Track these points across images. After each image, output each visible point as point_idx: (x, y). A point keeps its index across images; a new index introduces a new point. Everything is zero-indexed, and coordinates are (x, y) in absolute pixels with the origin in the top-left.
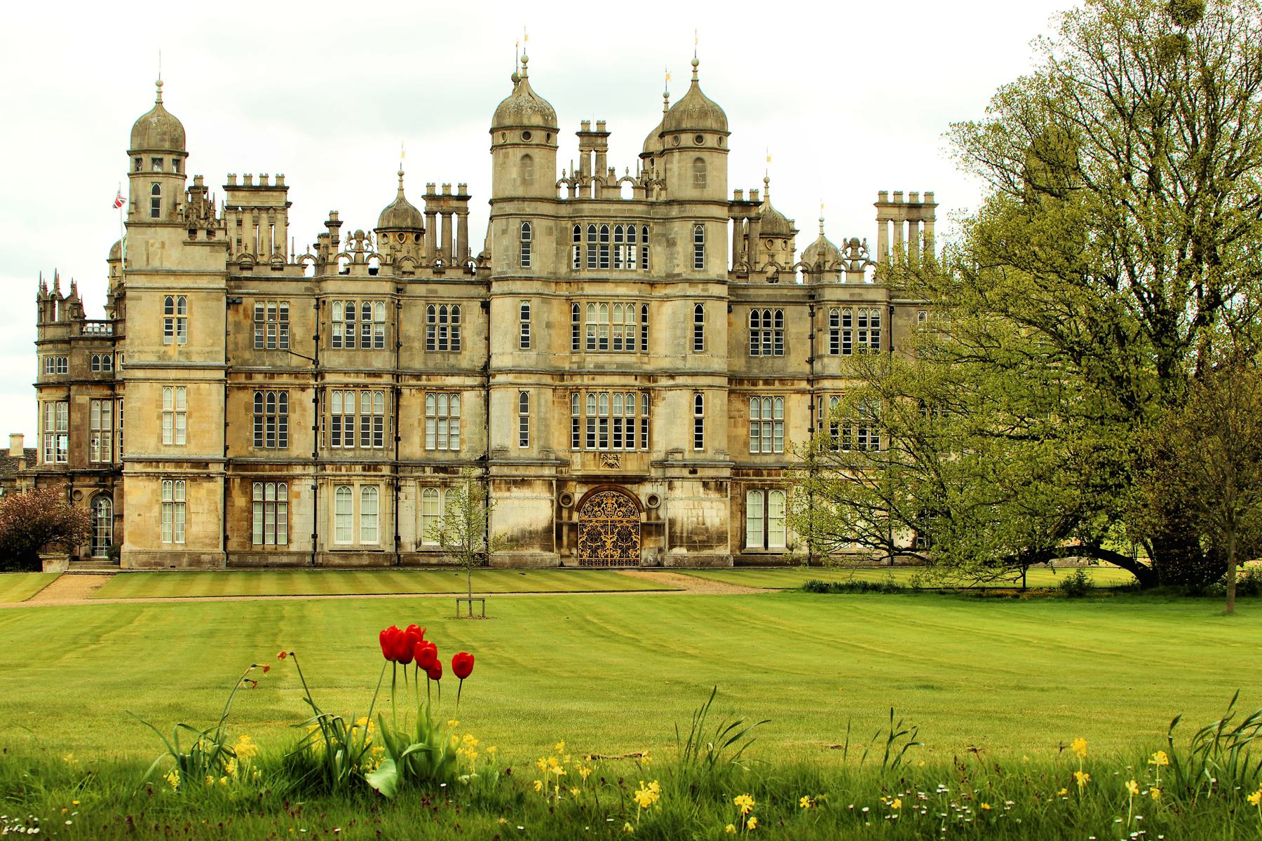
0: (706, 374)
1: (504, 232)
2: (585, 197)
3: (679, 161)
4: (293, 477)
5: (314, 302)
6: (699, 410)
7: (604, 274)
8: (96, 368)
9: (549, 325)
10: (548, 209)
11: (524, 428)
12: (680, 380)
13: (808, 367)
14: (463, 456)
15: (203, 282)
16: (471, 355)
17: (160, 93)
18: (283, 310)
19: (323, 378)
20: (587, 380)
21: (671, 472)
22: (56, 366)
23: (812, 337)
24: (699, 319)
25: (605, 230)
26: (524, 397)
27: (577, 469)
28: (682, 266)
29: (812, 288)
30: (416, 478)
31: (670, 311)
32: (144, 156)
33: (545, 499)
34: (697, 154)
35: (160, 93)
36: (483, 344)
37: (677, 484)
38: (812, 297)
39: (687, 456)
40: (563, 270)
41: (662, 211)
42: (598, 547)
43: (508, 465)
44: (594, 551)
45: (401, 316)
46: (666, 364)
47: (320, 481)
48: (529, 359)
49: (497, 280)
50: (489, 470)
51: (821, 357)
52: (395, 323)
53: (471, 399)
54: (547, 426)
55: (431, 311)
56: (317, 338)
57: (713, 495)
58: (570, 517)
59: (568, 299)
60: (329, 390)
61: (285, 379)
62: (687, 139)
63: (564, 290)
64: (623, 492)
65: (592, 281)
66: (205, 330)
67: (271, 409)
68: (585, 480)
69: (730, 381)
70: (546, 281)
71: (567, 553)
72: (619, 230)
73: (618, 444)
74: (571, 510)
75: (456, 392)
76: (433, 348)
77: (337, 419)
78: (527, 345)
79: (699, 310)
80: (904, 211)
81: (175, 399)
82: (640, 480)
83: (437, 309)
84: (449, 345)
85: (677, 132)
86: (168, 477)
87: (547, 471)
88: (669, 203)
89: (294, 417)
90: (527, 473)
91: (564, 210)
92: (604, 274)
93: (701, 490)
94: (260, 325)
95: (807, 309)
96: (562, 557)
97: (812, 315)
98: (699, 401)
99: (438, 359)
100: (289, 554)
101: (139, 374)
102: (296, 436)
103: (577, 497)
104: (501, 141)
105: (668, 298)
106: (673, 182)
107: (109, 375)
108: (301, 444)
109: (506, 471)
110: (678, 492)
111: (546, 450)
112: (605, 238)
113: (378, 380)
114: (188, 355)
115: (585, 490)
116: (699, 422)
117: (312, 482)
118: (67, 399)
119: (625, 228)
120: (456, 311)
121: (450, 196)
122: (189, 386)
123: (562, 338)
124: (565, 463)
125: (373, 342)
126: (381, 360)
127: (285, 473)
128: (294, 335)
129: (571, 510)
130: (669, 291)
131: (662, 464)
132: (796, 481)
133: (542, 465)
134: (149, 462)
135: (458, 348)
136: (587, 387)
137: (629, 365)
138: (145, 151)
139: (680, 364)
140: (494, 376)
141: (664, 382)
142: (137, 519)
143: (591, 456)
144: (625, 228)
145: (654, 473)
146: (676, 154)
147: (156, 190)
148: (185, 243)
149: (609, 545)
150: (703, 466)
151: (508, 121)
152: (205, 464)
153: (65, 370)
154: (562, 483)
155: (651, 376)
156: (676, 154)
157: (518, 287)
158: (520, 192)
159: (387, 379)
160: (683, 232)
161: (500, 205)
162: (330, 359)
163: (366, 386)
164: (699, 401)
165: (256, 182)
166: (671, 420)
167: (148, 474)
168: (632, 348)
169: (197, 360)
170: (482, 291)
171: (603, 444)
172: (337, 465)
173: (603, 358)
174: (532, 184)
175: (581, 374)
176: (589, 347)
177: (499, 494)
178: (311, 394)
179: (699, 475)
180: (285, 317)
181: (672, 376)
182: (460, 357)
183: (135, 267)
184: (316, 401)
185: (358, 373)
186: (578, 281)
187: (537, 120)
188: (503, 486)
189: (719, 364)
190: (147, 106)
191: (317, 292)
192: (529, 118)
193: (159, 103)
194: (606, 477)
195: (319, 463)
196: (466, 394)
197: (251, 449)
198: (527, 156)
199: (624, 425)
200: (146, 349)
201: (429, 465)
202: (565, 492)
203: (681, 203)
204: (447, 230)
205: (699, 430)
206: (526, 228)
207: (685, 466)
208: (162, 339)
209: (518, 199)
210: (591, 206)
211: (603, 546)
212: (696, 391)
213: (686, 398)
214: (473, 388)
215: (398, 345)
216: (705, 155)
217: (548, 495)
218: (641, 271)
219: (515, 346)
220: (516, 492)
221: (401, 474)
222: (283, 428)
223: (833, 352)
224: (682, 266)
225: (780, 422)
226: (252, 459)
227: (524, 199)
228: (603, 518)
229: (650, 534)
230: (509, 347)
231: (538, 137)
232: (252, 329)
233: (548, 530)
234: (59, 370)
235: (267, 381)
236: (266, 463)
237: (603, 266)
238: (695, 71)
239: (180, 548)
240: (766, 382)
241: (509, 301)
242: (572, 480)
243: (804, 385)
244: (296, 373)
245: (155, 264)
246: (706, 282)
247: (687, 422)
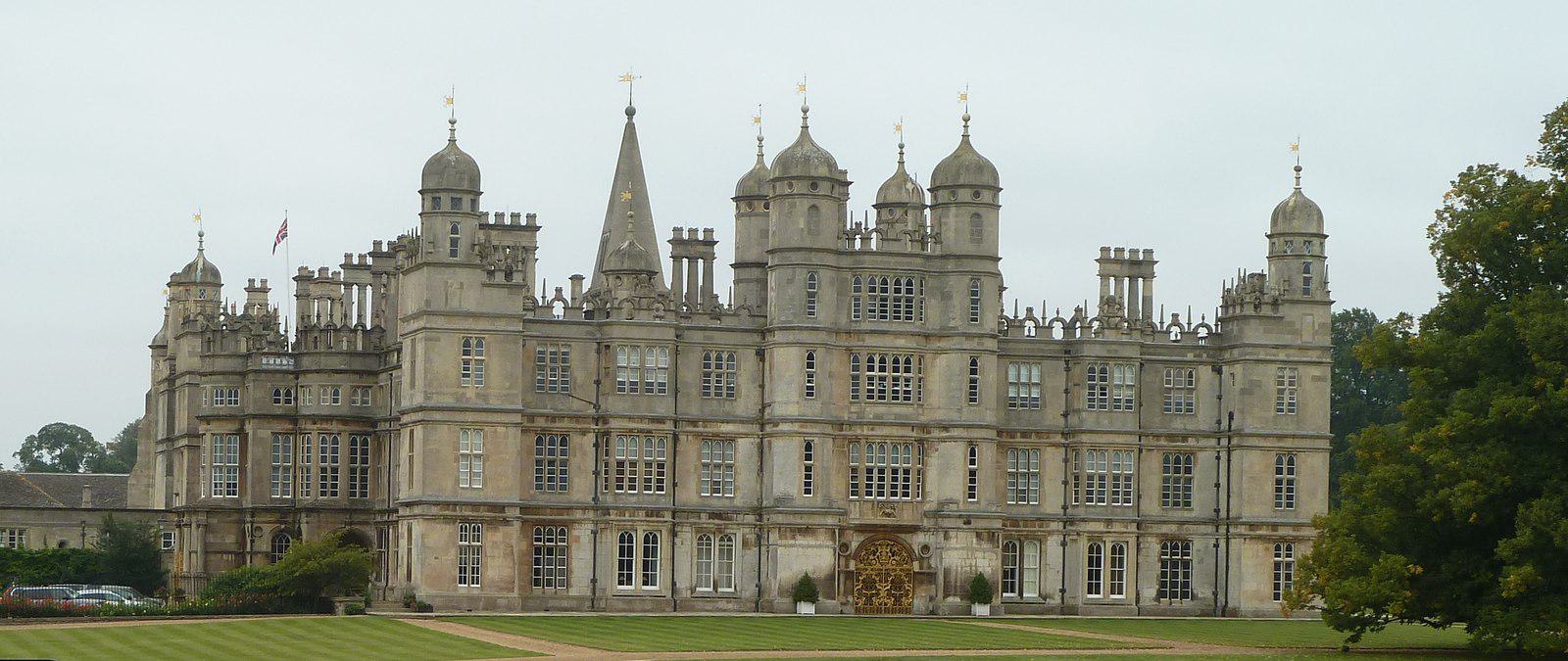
0: (981, 427)
1: (790, 281)
2: (866, 248)
4: (574, 522)
5: (595, 346)
6: (972, 462)
7: (884, 326)
8: (277, 401)
9: (831, 375)
10: (830, 259)
11: (808, 477)
12: (955, 432)
13: (1062, 421)
14: (738, 502)
15: (501, 325)
16: (746, 403)
17: (453, 130)
18: (564, 354)
19: (605, 422)
20: (866, 431)
21: (946, 523)
22: (226, 398)
23: (1067, 391)
24: (974, 372)
25: (885, 282)
26: (808, 447)
27: (855, 517)
28: (958, 320)
29: (1068, 343)
30: (691, 524)
31: (944, 363)
32: (443, 196)
33: (828, 547)
34: (974, 210)
35: (453, 130)
36: (756, 392)
37: (952, 534)
38: (1067, 352)
39: (961, 506)
40: (843, 321)
41: (936, 265)
42: (872, 595)
43: (795, 513)
44: (869, 599)
45: (679, 362)
46: (940, 415)
47: (603, 526)
48: (813, 408)
49: (780, 329)
50: (766, 519)
51: (1078, 411)
52: (675, 371)
53: (745, 447)
54: (828, 475)
55: (707, 358)
56: (598, 382)
57: (986, 545)
58: (847, 566)
59: (849, 350)
60: (613, 435)
61: (566, 424)
62: (965, 195)
63: (844, 341)
64: (897, 542)
65: (873, 332)
66: (501, 375)
67: (551, 452)
68: (861, 529)
69: (1000, 433)
70: (828, 331)
71: (844, 601)
72: (898, 282)
73: (894, 494)
74: (848, 558)
75: (731, 439)
76: (708, 394)
77: (620, 464)
78: (812, 394)
79: (974, 363)
80: (1126, 269)
81: (471, 444)
82: (914, 529)
83: (713, 355)
84: (724, 392)
85: (953, 188)
86: (465, 520)
87: (830, 520)
88: (943, 257)
89: (575, 461)
90: (811, 521)
91: (846, 261)
92: (884, 326)
93: (975, 540)
94: (542, 368)
95: (1063, 364)
96: (841, 604)
97: (1068, 369)
98: (973, 453)
99: (714, 407)
100: (569, 598)
101: (438, 416)
102: (576, 480)
103: (854, 545)
104: (788, 191)
105: (943, 351)
106: (949, 235)
107: (291, 409)
108: (581, 488)
109: (791, 519)
110: (953, 542)
111: (827, 497)
112: (884, 290)
113: (661, 426)
114: (485, 397)
115: (862, 538)
116: (973, 473)
117: (591, 526)
118: (241, 433)
119: (903, 281)
120: (731, 358)
121: (697, 240)
122: (486, 429)
123: (841, 388)
124: (845, 513)
125: (655, 387)
126: (663, 407)
127: (565, 517)
128: (576, 379)
129: (848, 558)
130: (943, 344)
131: (937, 514)
132: (1051, 533)
133: (826, 514)
134: (447, 505)
135: (732, 395)
136: (867, 437)
137: (906, 416)
138: (444, 190)
139: (954, 416)
140: (776, 425)
141: (936, 433)
142: (434, 562)
143: (870, 505)
144: (903, 281)
145: (926, 523)
146: (953, 210)
147: (454, 230)
148: (484, 285)
149: (883, 594)
150: (978, 517)
151: (794, 173)
152: (502, 508)
153: (236, 402)
154: (842, 530)
155: (925, 427)
156: (953, 210)
157: (805, 336)
158: (808, 244)
159: (669, 426)
160: (959, 286)
162: (613, 404)
163: (650, 431)
164: (973, 453)
165: (507, 221)
166: (944, 470)
167: (445, 518)
168: (909, 399)
169: (494, 403)
170: (757, 338)
171: (881, 494)
172: (621, 511)
173: (881, 409)
174: (818, 234)
175: (861, 424)
176: (869, 397)
177: (784, 542)
178: (591, 438)
179: (972, 526)
180: (564, 361)
181: (946, 428)
182: (735, 403)
183: (434, 307)
184: (596, 445)
185: (642, 419)
186: (860, 332)
187: (823, 171)
188: (788, 534)
189: (990, 418)
190: (441, 145)
191: (598, 335)
192: (816, 167)
193: (452, 141)
194: (884, 526)
195: (599, 508)
196: (740, 441)
197: (532, 492)
198: (814, 206)
199: (900, 475)
200: (446, 390)
201: (705, 511)
202: (843, 541)
203: (958, 257)
204: (693, 274)
205: (973, 481)
206: (812, 278)
207: (960, 516)
208: (459, 379)
209: (806, 249)
210: (872, 258)
211: (877, 594)
212: (971, 443)
213: (959, 451)
214: (746, 435)
215: (677, 391)
216: (982, 211)
217: (831, 543)
218: (918, 323)
219: (800, 395)
220: (801, 540)
221: (677, 520)
222: (564, 472)
223: (1090, 406)
224: (958, 320)
225: (1035, 475)
226: (534, 503)
227: (811, 250)
228: (878, 566)
229: (922, 583)
230: (795, 397)
231: (824, 188)
232: (534, 370)
233: (831, 578)
234: (230, 402)
235: (550, 425)
236: (546, 507)
237: (907, 318)
238: (966, 127)
239: (476, 592)
240: (1025, 434)
241: (794, 351)
242: (850, 528)
243: (1059, 439)
244: (577, 418)
245: (454, 304)
246: (982, 336)
247: (961, 473)
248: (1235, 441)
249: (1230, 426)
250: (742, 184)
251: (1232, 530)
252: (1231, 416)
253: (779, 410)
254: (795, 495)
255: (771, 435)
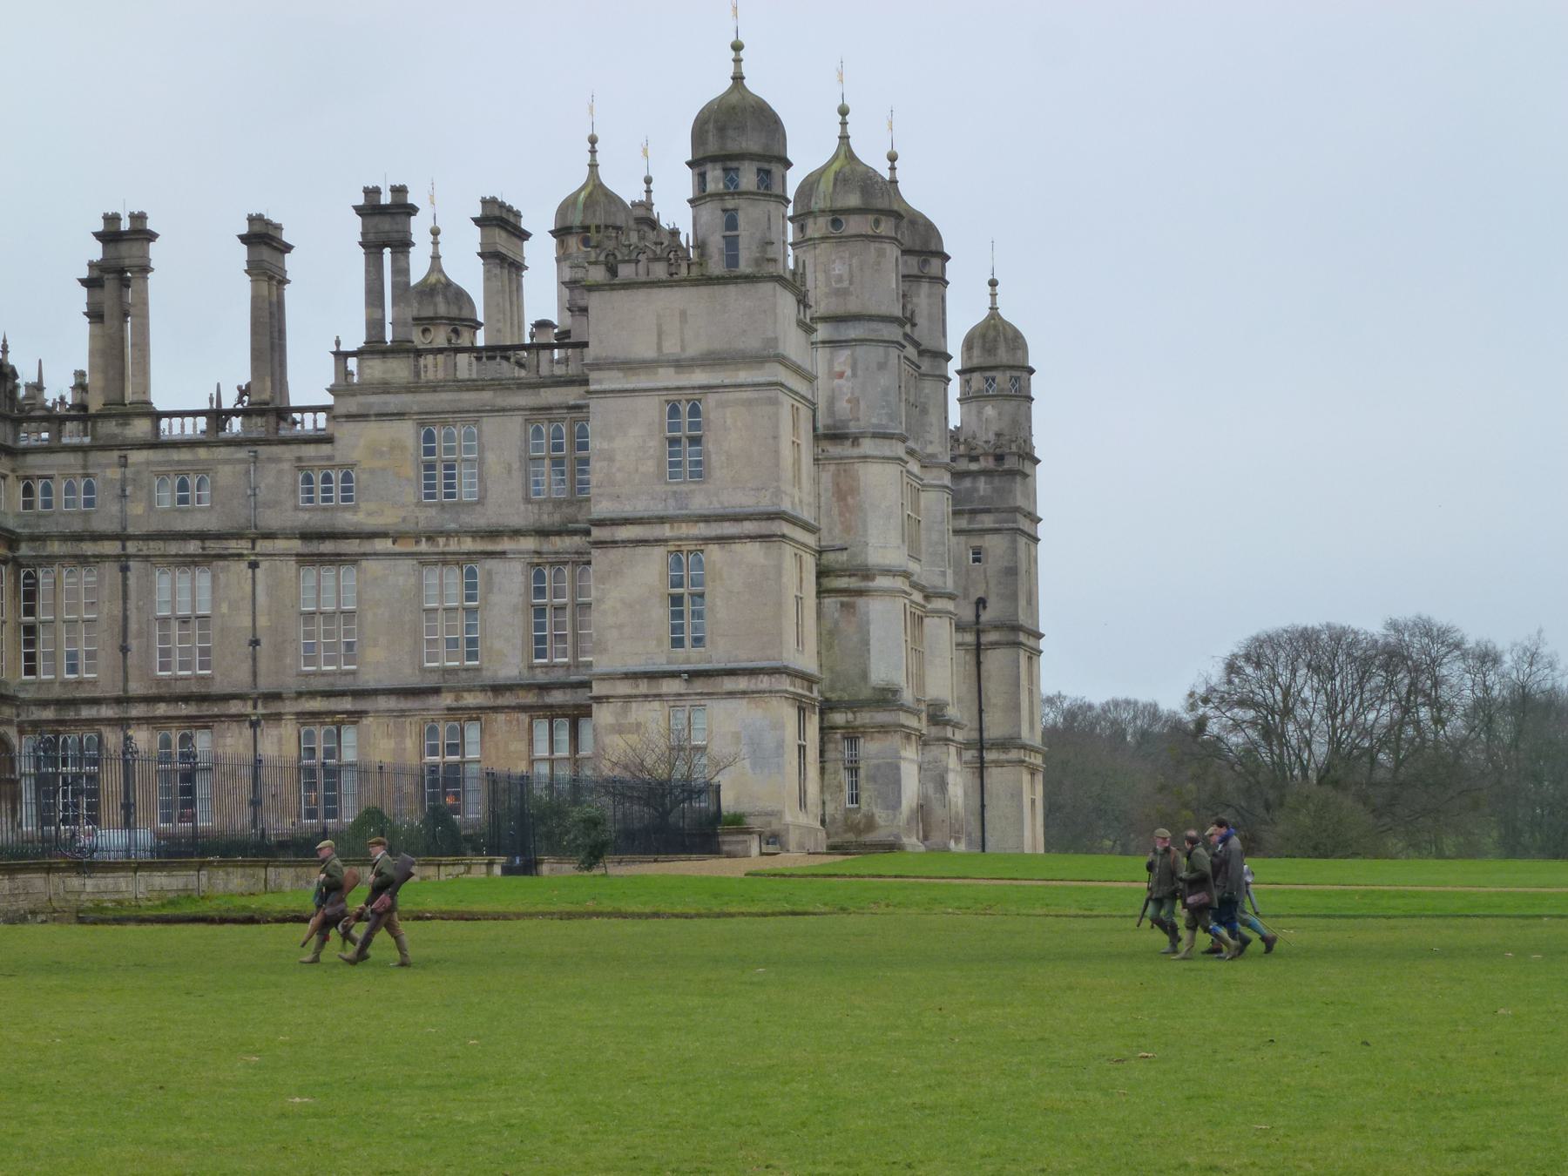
1: (882, 366)
3: (930, 296)
17: (737, 61)
35: (737, 61)
49: (875, 436)
101: (787, 529)
140: (873, 579)
161: (874, 325)
193: (738, 78)
230: (894, 537)
241: (893, 470)
248: (988, 638)
249: (978, 616)
250: (565, 208)
251: (990, 756)
252: (981, 603)
253: (875, 557)
254: (903, 684)
255: (860, 593)
